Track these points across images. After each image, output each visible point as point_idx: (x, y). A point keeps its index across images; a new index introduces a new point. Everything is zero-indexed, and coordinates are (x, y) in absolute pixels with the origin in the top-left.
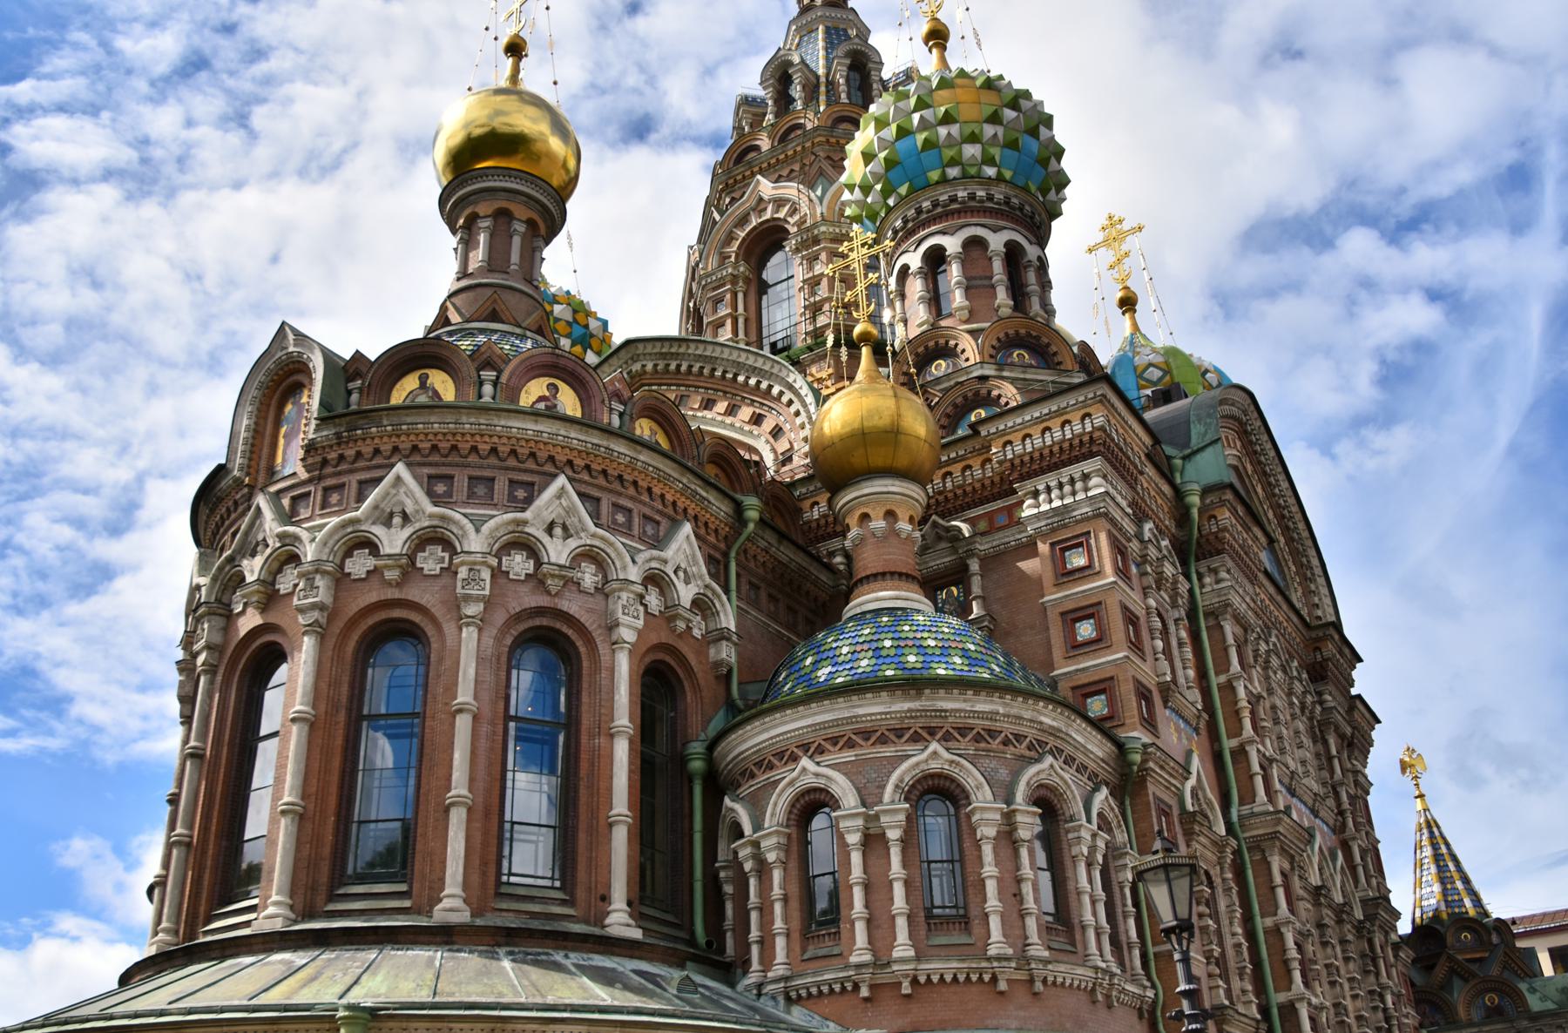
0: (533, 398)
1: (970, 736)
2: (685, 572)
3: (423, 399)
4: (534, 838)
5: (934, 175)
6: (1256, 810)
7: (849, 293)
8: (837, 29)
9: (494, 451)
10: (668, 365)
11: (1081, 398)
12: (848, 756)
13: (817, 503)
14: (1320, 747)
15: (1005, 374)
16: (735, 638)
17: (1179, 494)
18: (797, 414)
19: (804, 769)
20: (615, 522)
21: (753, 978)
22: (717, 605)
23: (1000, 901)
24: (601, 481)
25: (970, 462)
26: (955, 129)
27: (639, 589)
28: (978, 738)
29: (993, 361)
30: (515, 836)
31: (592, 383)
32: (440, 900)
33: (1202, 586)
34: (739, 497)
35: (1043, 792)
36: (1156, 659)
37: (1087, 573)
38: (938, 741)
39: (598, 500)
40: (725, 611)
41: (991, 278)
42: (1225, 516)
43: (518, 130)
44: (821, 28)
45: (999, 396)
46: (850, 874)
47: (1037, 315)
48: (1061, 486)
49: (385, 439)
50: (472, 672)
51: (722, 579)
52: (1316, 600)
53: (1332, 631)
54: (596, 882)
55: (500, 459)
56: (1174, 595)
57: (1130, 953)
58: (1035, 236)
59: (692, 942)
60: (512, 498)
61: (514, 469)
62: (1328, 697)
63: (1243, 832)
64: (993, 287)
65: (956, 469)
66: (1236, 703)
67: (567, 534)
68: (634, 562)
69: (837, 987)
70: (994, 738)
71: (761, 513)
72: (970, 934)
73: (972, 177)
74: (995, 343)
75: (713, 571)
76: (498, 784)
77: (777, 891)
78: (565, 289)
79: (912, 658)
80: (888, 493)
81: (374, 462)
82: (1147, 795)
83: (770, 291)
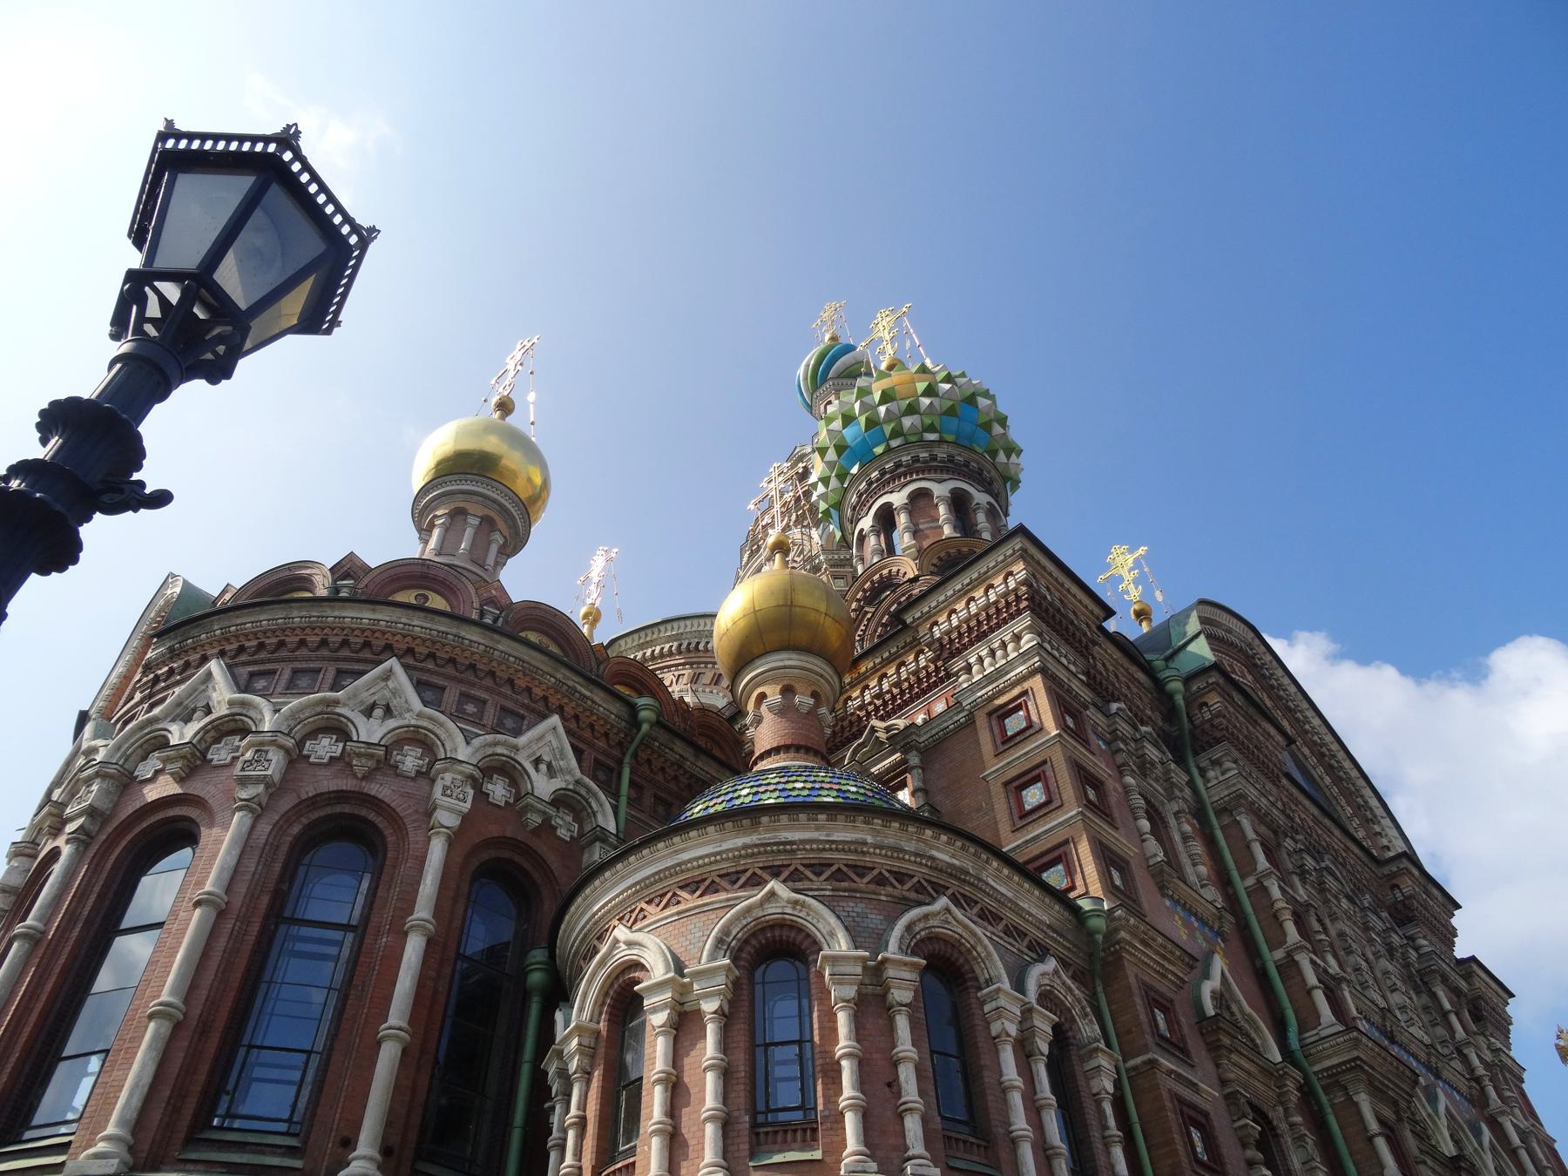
2: (549, 766)
5: (879, 450)
11: (1002, 558)
14: (1425, 999)
16: (613, 840)
17: (1159, 685)
22: (594, 805)
24: (450, 670)
28: (839, 876)
36: (1143, 841)
39: (443, 689)
42: (1215, 701)
52: (1385, 842)
53: (1405, 863)
56: (1170, 786)
61: (345, 659)
63: (1312, 1064)
67: (388, 712)
68: (468, 743)
70: (862, 876)
71: (658, 716)
74: (935, 561)
80: (785, 667)
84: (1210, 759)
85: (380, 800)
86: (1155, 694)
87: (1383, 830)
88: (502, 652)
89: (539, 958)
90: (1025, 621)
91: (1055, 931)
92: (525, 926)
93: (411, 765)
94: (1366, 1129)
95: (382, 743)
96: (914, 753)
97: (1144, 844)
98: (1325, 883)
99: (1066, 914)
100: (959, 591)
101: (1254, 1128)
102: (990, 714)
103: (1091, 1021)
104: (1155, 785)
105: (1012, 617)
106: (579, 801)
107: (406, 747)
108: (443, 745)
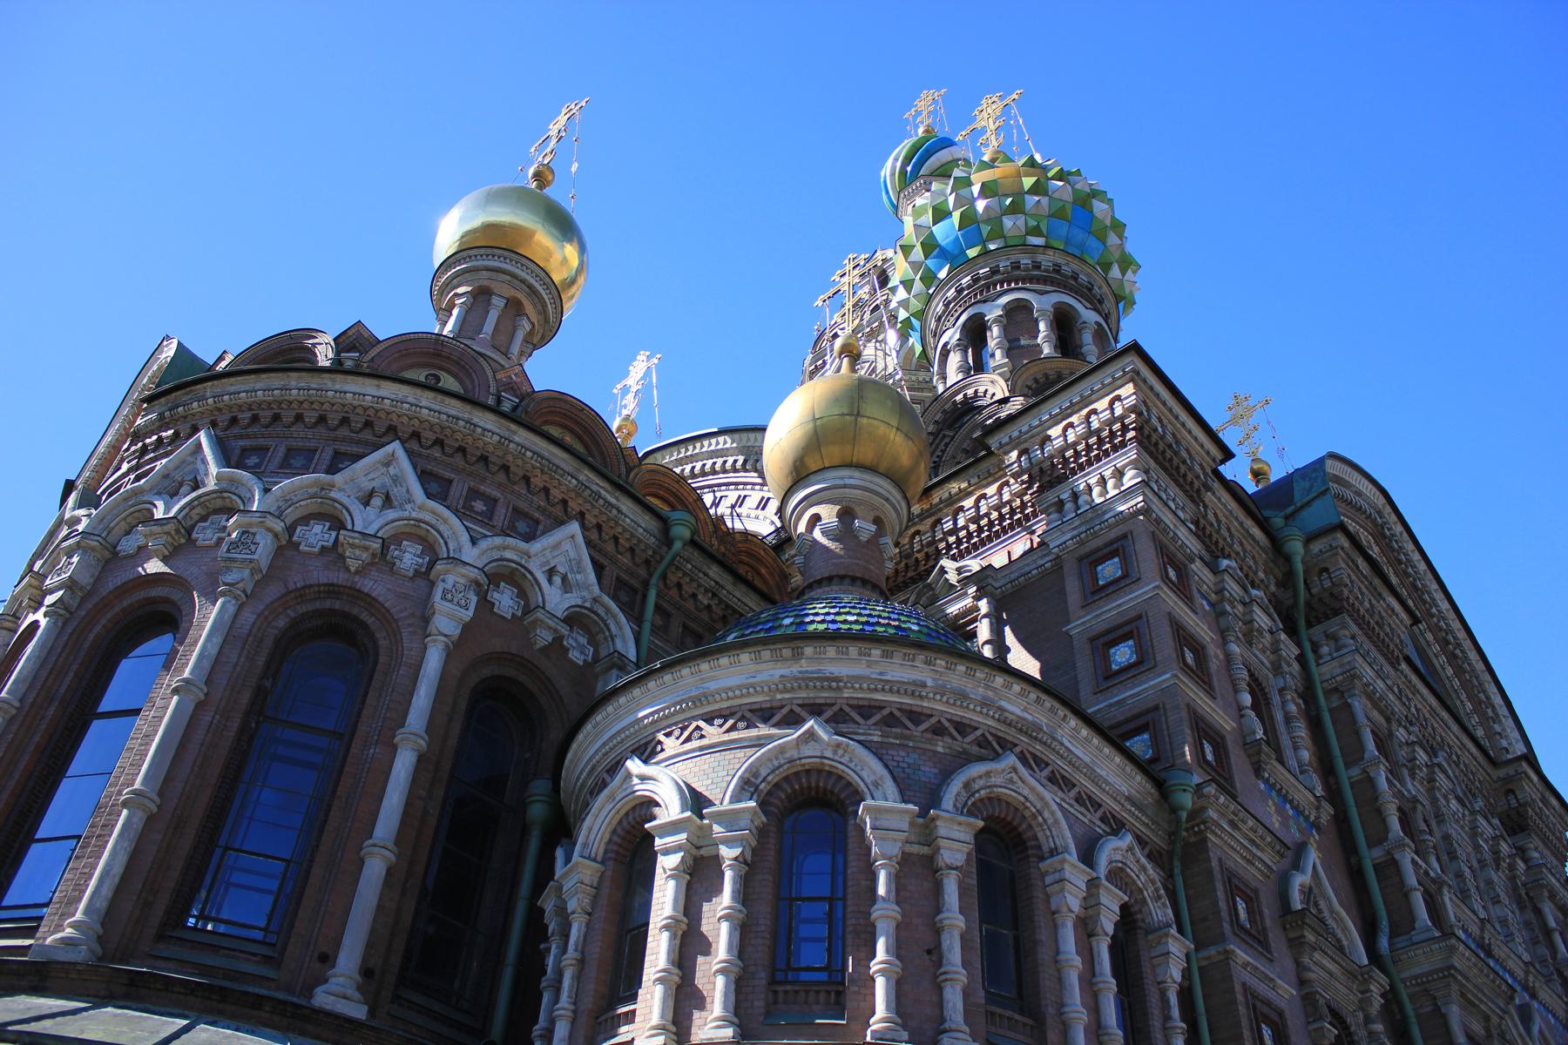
1: (877, 717)
2: (564, 579)
5: (972, 253)
6: (1415, 939)
22: (613, 628)
24: (458, 460)
33: (1318, 656)
36: (1242, 716)
52: (1504, 743)
61: (344, 440)
66: (1377, 798)
67: (388, 502)
70: (917, 723)
71: (693, 534)
80: (845, 486)
82: (1209, 860)
84: (1325, 632)
85: (374, 599)
86: (1270, 554)
87: (1504, 730)
88: (518, 444)
90: (1131, 453)
91: (1134, 804)
92: (528, 755)
93: (409, 562)
95: (379, 535)
97: (1243, 720)
98: (1435, 780)
99: (1149, 786)
101: (1331, 1031)
103: (1164, 905)
104: (1261, 656)
105: (1115, 448)
107: (405, 543)
108: (446, 543)
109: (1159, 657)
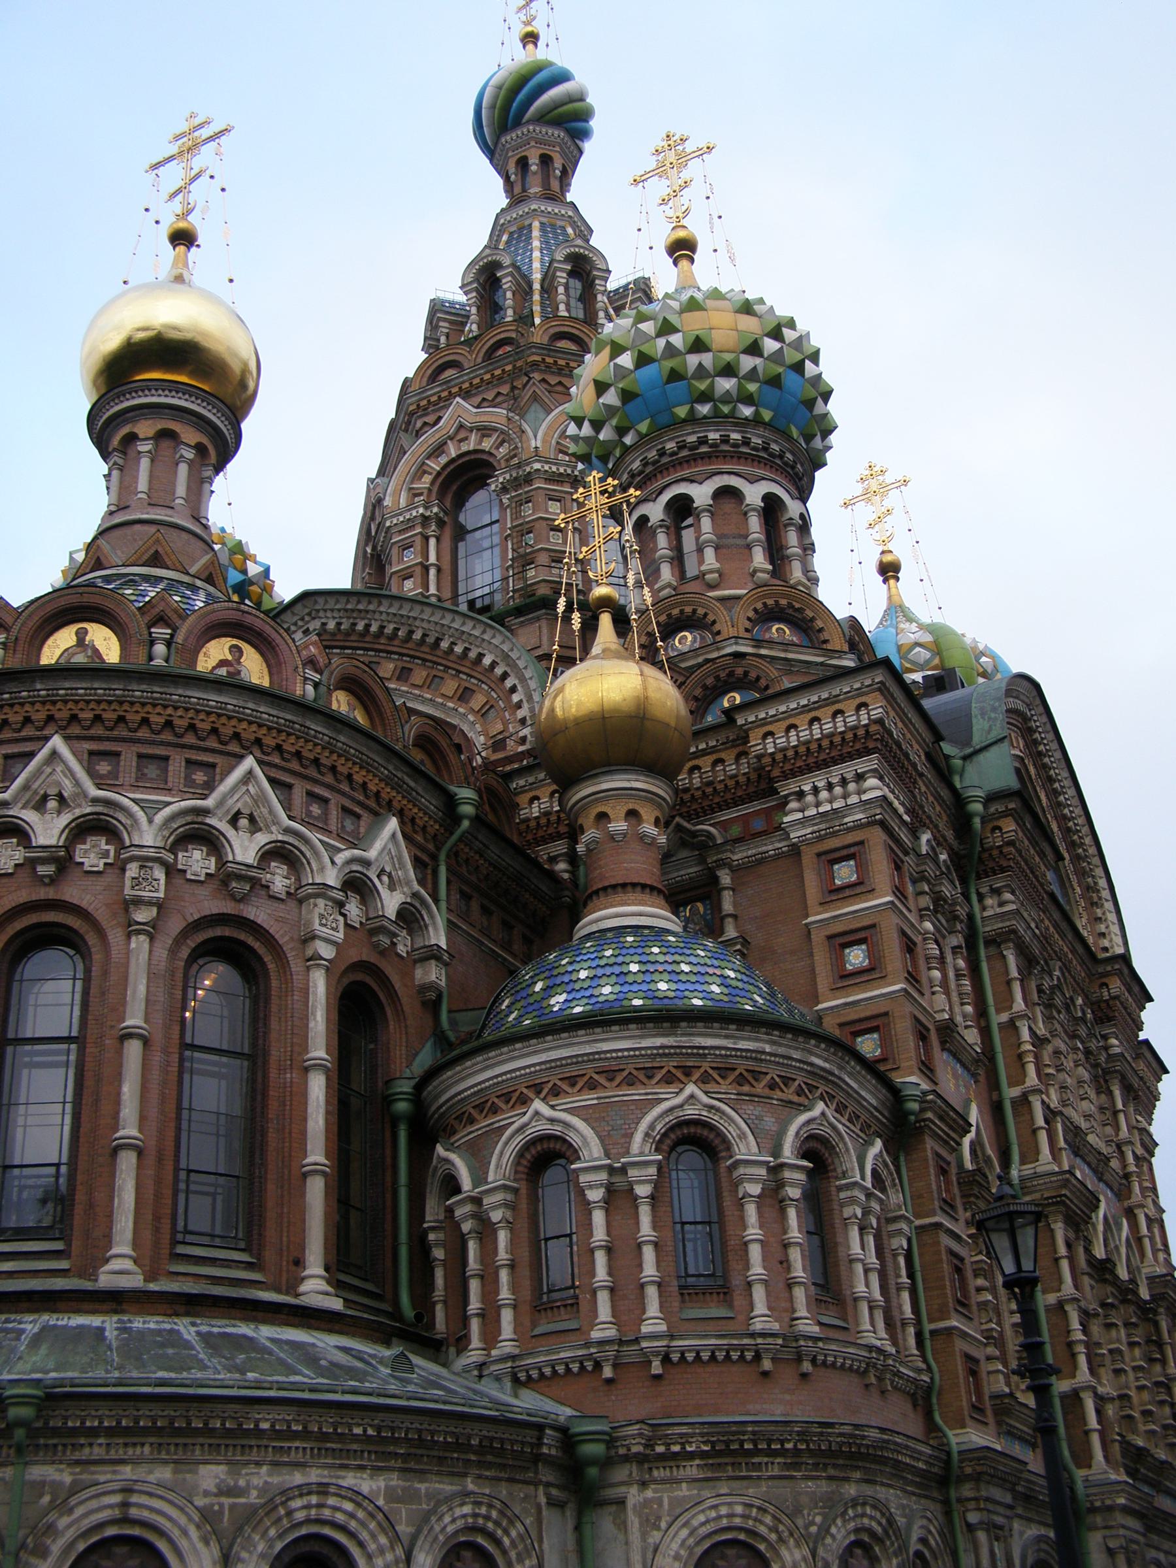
0: (212, 663)
1: (732, 1077)
2: (390, 876)
3: (80, 659)
4: (212, 1189)
5: (682, 412)
6: (1039, 1170)
7: (584, 549)
8: (553, 226)
9: (169, 724)
10: (354, 624)
12: (589, 1099)
13: (537, 798)
15: (763, 652)
16: (446, 957)
17: (959, 801)
18: (513, 689)
19: (537, 1113)
20: (309, 813)
21: (474, 1356)
23: (765, 1268)
24: (294, 765)
25: (723, 755)
26: (707, 359)
27: (339, 896)
28: (741, 1080)
29: (748, 635)
30: (193, 1187)
31: (283, 646)
32: (107, 1261)
33: (984, 909)
34: (453, 788)
35: (813, 1144)
36: (933, 993)
37: (859, 890)
38: (695, 1083)
39: (290, 787)
40: (434, 923)
41: (747, 537)
42: (1009, 826)
43: (188, 336)
44: (536, 224)
45: (758, 678)
46: (591, 1235)
47: (800, 583)
48: (830, 787)
49: (38, 706)
50: (142, 989)
51: (430, 886)
54: (289, 1242)
55: (176, 735)
57: (904, 1331)
58: (798, 488)
59: (397, 1314)
60: (189, 782)
61: (191, 747)
62: (1114, 1041)
64: (749, 547)
65: (706, 762)
67: (255, 825)
68: (333, 862)
69: (575, 1367)
72: (730, 1305)
73: (726, 416)
74: (751, 614)
75: (420, 876)
76: (173, 1124)
77: (503, 1255)
78: (220, 526)
79: (663, 986)
81: (23, 734)
82: (925, 1150)
83: (468, 537)
84: (991, 886)
85: (259, 925)
87: (1104, 914)
89: (405, 1090)
92: (372, 1046)
93: (280, 885)
94: (1055, 1252)
96: (727, 871)
99: (888, 1095)
100: (804, 706)
102: (819, 855)
105: (860, 754)
106: (413, 914)
107: (273, 864)
108: (309, 863)
109: (889, 968)
